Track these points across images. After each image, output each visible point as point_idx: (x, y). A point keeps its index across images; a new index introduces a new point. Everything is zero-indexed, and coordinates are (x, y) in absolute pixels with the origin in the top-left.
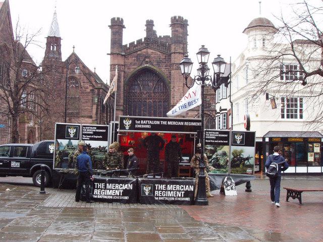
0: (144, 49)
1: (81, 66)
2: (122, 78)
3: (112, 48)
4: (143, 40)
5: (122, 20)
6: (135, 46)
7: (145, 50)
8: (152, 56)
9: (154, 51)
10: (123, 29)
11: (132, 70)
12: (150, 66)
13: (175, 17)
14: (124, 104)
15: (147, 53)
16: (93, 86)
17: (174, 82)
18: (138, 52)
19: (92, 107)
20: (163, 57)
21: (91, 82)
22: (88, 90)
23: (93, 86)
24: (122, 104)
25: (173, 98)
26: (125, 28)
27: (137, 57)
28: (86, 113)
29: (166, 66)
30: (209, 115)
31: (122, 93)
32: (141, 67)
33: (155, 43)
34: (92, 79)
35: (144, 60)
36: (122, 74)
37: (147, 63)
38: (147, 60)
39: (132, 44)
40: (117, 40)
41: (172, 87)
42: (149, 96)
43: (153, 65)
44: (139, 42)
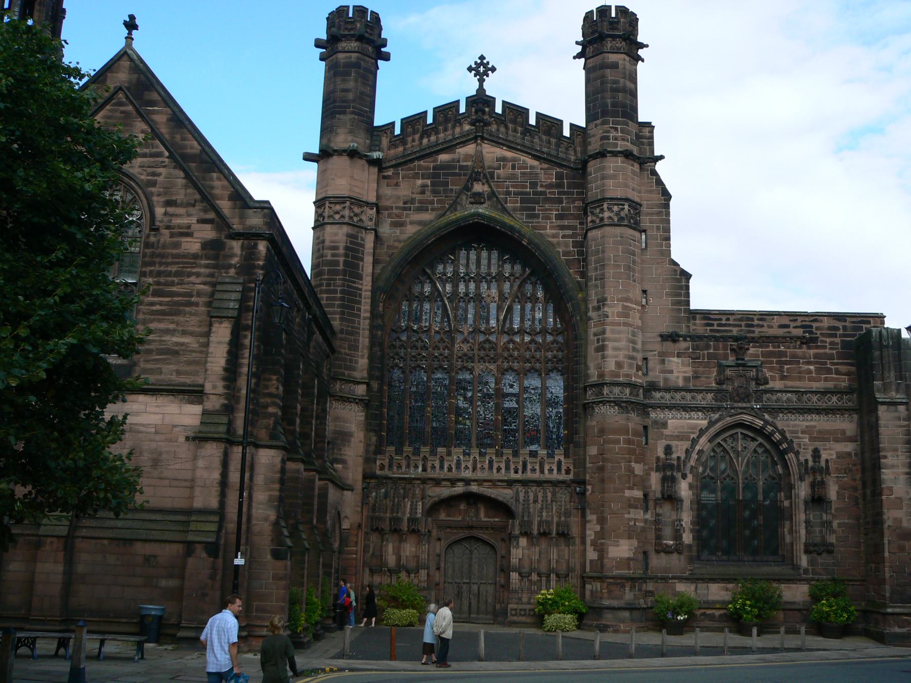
0: (464, 143)
1: (161, 118)
2: (368, 259)
3: (327, 129)
4: (462, 109)
5: (376, 18)
6: (428, 131)
7: (470, 149)
8: (501, 172)
9: (509, 154)
10: (380, 62)
11: (411, 230)
12: (494, 214)
13: (604, 11)
14: (371, 376)
15: (479, 158)
16: (221, 222)
17: (602, 278)
18: (444, 157)
19: (208, 334)
20: (547, 176)
21: (207, 200)
22: (192, 246)
23: (221, 222)
24: (365, 374)
25: (601, 349)
26: (386, 57)
27: (435, 176)
28: (169, 373)
29: (559, 217)
30: (760, 432)
31: (364, 324)
32: (452, 217)
33: (514, 122)
34: (218, 185)
35: (467, 188)
36: (369, 240)
37: (478, 199)
38: (478, 187)
39: (413, 122)
40: (351, 96)
41: (593, 303)
42: (482, 348)
43: (504, 210)
44: (447, 112)
